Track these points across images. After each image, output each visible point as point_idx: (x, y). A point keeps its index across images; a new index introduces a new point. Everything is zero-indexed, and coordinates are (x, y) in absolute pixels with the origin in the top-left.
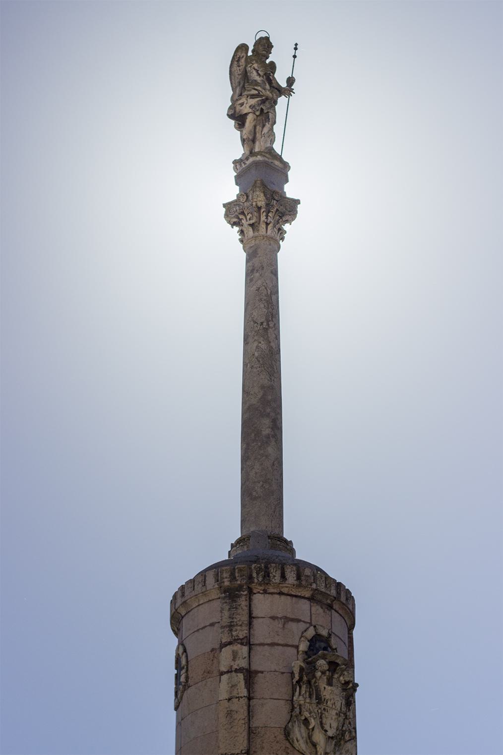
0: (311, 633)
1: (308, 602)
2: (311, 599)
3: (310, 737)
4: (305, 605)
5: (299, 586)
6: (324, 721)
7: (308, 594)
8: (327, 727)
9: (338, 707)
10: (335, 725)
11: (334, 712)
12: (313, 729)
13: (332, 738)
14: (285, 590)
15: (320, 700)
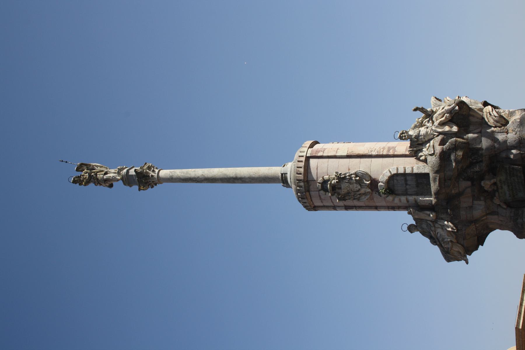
0: (322, 192)
1: (311, 193)
2: (309, 191)
3: (364, 194)
4: (312, 193)
5: (307, 198)
6: (355, 190)
7: (308, 193)
8: (357, 189)
9: (347, 185)
10: (355, 185)
11: (351, 186)
12: (360, 194)
13: (360, 185)
14: (310, 200)
15: (348, 193)
